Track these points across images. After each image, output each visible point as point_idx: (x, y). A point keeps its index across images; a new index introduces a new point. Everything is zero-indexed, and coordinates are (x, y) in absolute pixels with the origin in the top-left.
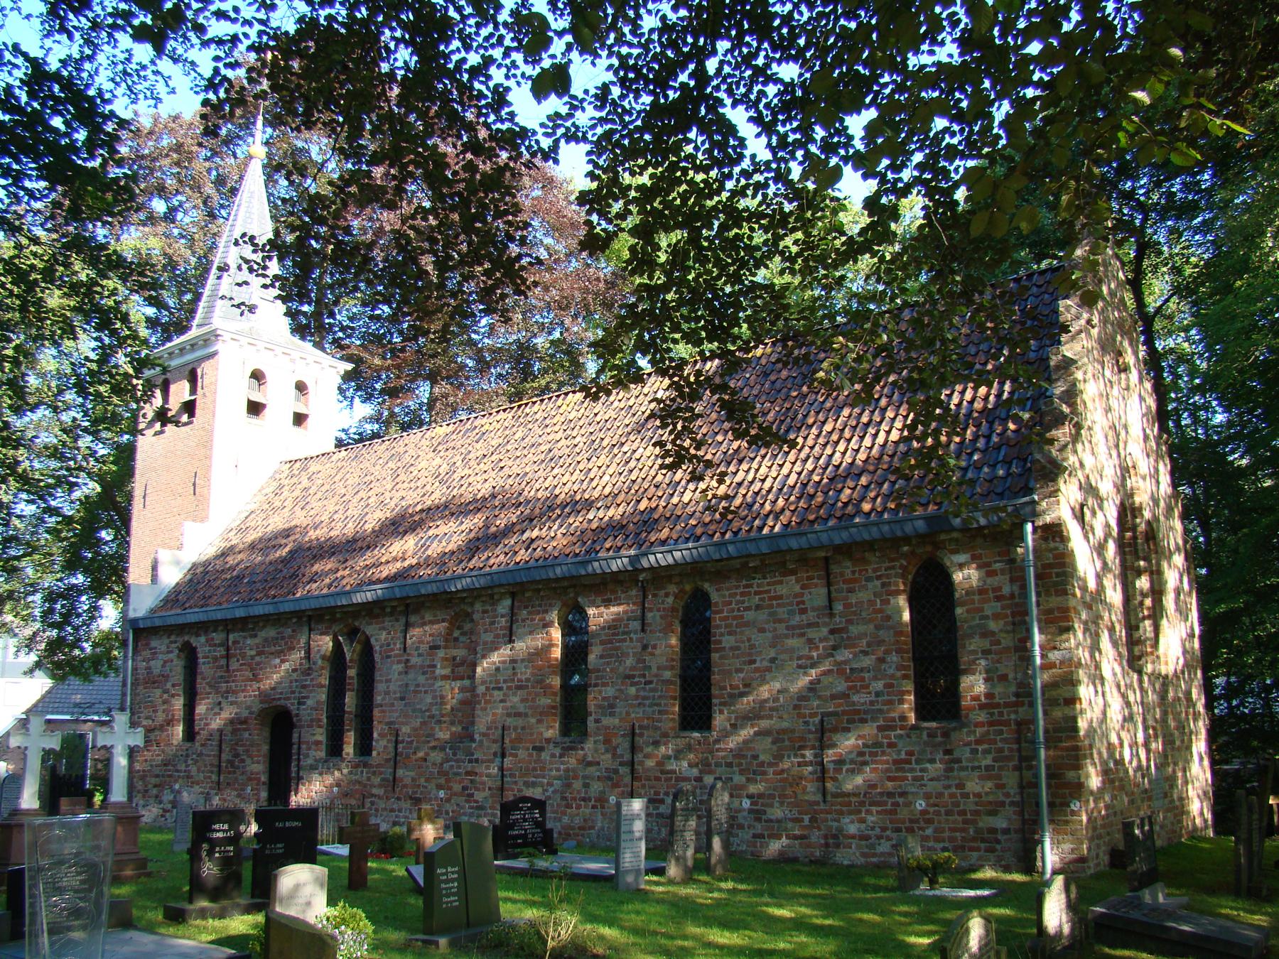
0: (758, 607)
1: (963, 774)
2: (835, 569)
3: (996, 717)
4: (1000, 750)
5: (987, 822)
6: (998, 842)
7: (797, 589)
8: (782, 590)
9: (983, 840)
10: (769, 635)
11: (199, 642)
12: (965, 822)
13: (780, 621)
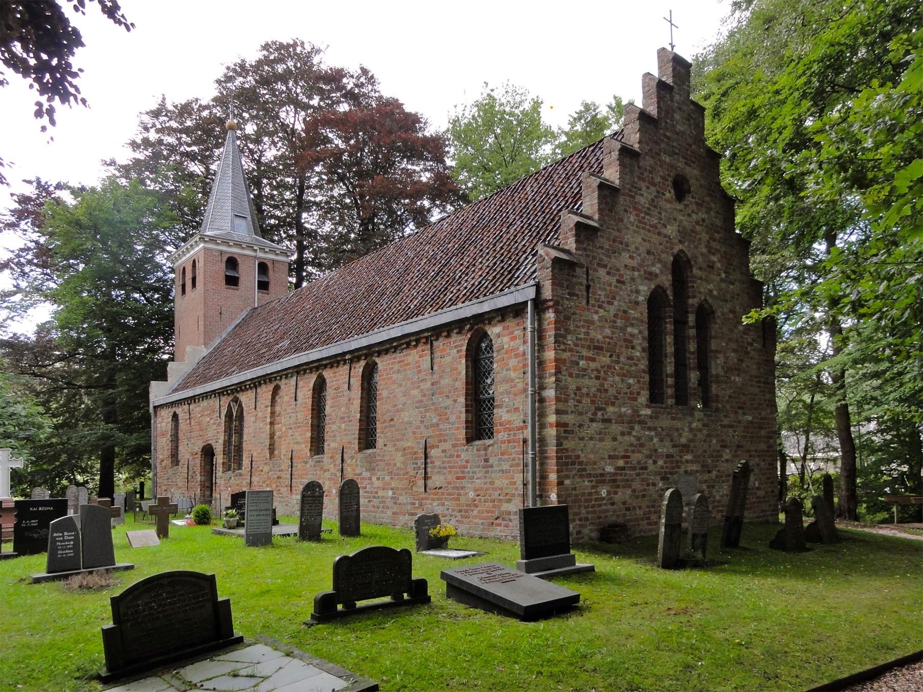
1: (493, 475)
3: (512, 437)
4: (514, 460)
5: (505, 507)
6: (510, 520)
9: (503, 519)
10: (403, 388)
11: (179, 410)
12: (494, 507)
13: (409, 379)
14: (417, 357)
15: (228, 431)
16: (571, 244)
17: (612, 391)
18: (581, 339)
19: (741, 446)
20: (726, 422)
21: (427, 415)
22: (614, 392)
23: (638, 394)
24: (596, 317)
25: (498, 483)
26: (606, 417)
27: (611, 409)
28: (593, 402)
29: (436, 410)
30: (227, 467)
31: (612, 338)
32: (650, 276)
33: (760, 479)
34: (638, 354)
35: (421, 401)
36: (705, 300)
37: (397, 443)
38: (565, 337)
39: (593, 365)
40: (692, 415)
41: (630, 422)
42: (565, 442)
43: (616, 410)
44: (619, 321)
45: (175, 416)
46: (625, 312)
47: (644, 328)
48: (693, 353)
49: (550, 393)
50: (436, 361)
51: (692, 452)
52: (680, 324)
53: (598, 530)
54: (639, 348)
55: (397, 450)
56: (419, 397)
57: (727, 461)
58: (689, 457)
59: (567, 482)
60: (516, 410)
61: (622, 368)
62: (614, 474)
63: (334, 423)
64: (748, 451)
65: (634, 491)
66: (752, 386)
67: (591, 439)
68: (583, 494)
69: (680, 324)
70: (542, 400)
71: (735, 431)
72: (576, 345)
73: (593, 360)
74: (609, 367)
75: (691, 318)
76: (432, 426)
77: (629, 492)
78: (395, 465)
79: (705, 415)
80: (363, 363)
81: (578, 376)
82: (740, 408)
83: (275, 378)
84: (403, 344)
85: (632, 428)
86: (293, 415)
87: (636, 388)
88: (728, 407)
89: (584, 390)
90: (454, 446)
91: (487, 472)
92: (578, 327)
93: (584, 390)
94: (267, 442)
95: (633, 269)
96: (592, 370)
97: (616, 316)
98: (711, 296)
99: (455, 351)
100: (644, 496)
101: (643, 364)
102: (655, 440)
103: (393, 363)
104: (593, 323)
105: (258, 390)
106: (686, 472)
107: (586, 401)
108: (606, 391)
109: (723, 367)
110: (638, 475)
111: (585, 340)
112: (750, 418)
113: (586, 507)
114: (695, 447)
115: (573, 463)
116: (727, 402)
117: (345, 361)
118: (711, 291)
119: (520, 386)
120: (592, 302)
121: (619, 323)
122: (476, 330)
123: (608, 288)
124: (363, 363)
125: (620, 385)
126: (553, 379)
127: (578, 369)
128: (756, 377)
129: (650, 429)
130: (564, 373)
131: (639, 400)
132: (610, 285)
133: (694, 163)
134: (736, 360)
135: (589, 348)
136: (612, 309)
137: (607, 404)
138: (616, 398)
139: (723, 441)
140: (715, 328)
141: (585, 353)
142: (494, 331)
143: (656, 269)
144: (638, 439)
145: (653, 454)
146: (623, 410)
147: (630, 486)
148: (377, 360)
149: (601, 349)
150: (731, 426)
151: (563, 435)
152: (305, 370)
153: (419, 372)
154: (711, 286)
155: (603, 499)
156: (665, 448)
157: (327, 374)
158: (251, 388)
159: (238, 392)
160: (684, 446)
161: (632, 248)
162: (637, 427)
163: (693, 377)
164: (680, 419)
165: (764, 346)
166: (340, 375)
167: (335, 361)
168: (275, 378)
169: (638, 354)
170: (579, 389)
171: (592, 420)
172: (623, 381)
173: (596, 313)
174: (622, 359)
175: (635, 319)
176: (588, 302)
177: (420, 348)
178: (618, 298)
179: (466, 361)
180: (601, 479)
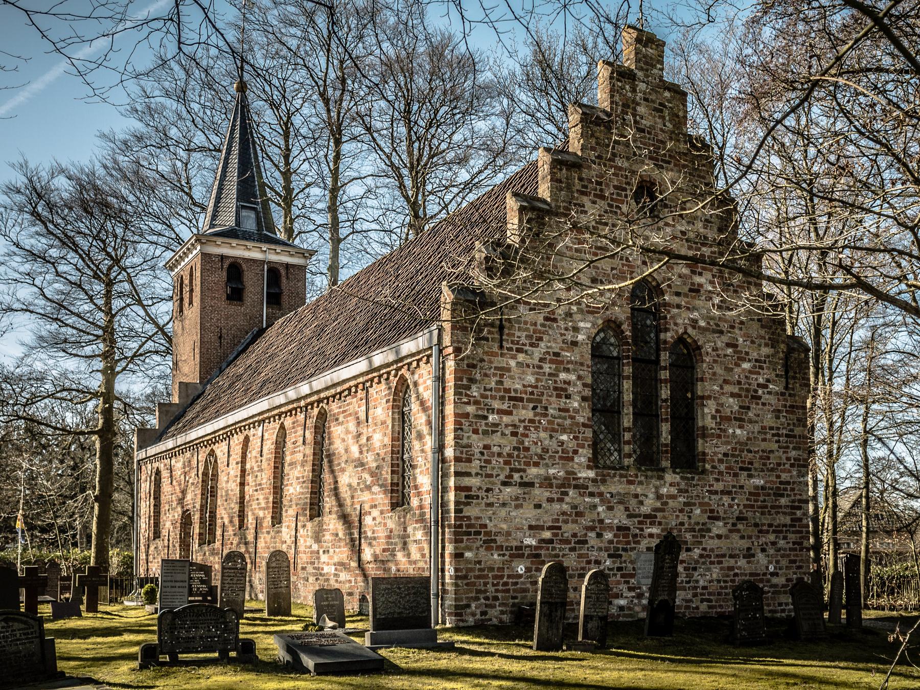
18: (491, 390)
19: (745, 519)
20: (719, 486)
22: (539, 451)
23: (576, 452)
24: (513, 363)
26: (525, 480)
27: (533, 471)
33: (777, 562)
34: (576, 405)
36: (686, 332)
39: (506, 419)
40: (661, 478)
41: (562, 486)
42: (465, 509)
43: (542, 471)
46: (557, 354)
48: (666, 401)
49: (449, 452)
50: (371, 412)
51: (660, 523)
53: (511, 612)
57: (719, 537)
59: (468, 554)
61: (549, 422)
62: (536, 548)
64: (756, 525)
66: (764, 440)
67: (504, 505)
68: (491, 569)
70: (444, 461)
71: (733, 499)
73: (509, 413)
79: (682, 478)
81: (485, 433)
87: (572, 445)
88: (722, 467)
89: (495, 449)
92: (486, 375)
93: (495, 449)
96: (506, 426)
97: (541, 360)
98: (694, 327)
102: (600, 509)
104: (509, 370)
108: (527, 449)
109: (714, 417)
110: (573, 549)
112: (761, 482)
113: (494, 585)
114: (664, 517)
115: (479, 533)
116: (721, 461)
118: (695, 321)
121: (547, 368)
123: (532, 328)
125: (547, 442)
127: (487, 424)
128: (771, 428)
129: (592, 495)
131: (576, 460)
132: (535, 324)
133: (669, 163)
134: (736, 408)
135: (502, 398)
136: (537, 353)
137: (527, 464)
138: (541, 457)
139: (712, 511)
141: (496, 405)
145: (598, 527)
146: (552, 471)
149: (521, 400)
150: (729, 493)
151: (463, 500)
154: (695, 315)
155: (520, 576)
156: (618, 517)
160: (646, 516)
164: (641, 483)
165: (786, 388)
169: (576, 405)
170: (486, 447)
171: (505, 484)
172: (551, 437)
173: (514, 357)
174: (551, 411)
176: (501, 347)
178: (545, 338)
180: (518, 552)
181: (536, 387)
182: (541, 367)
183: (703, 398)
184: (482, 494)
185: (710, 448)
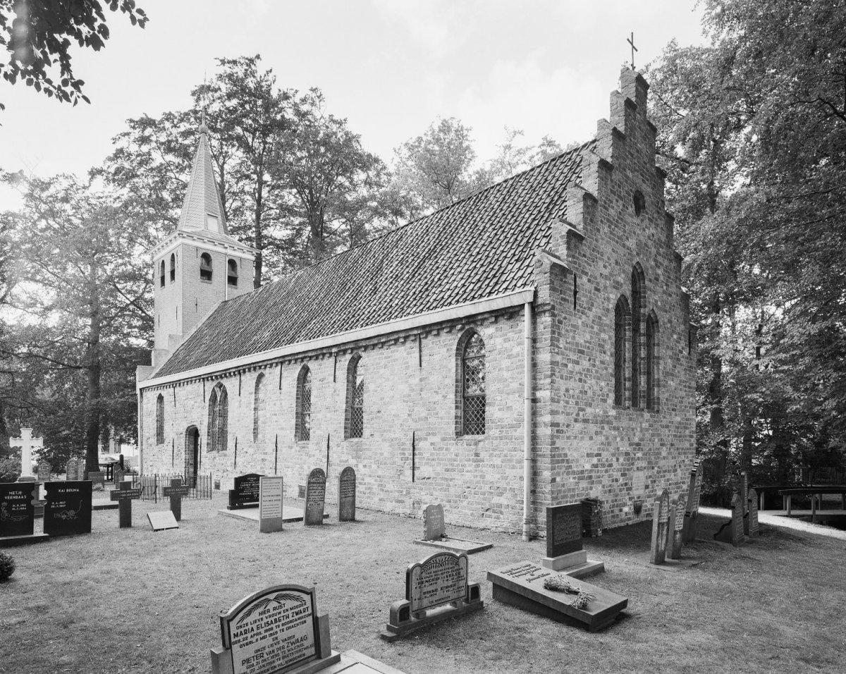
0: (385, 367)
2: (424, 341)
3: (504, 434)
6: (502, 513)
7: (405, 354)
8: (397, 355)
9: (494, 512)
14: (404, 354)
15: (212, 413)
16: (562, 251)
17: (590, 393)
21: (416, 409)
25: (489, 478)
27: (589, 410)
28: (577, 403)
29: (424, 405)
30: (212, 447)
31: (590, 343)
32: (617, 286)
34: (608, 358)
35: (410, 396)
37: (385, 434)
38: (558, 341)
39: (577, 368)
42: (557, 441)
44: (595, 327)
45: (160, 398)
47: (613, 334)
52: (636, 330)
54: (609, 354)
55: (384, 440)
56: (407, 392)
57: (664, 458)
58: (639, 455)
59: (558, 479)
60: (509, 408)
61: (597, 372)
62: (591, 471)
63: (318, 412)
65: (603, 486)
67: (575, 437)
68: (569, 490)
69: (636, 330)
72: (566, 349)
73: (577, 363)
74: (588, 370)
75: (643, 326)
76: (420, 419)
77: (600, 488)
78: (382, 454)
80: (348, 357)
82: (673, 410)
83: (260, 367)
84: (391, 340)
85: (603, 428)
86: (278, 403)
89: (571, 392)
90: (443, 439)
91: (478, 466)
92: (567, 331)
94: (252, 426)
95: (606, 278)
99: (445, 349)
100: (610, 490)
101: (611, 369)
102: (618, 439)
103: (379, 359)
105: (243, 378)
106: (638, 468)
107: (572, 401)
110: (606, 471)
111: (572, 344)
112: (678, 419)
117: (331, 354)
119: (515, 385)
120: (578, 307)
122: (468, 328)
124: (348, 357)
126: (549, 380)
130: (557, 374)
132: (590, 292)
136: (591, 314)
140: (658, 337)
141: (573, 357)
142: (486, 332)
143: (621, 279)
144: (607, 438)
146: (597, 410)
147: (600, 482)
148: (363, 354)
149: (582, 352)
150: (667, 427)
152: (290, 361)
153: (407, 368)
157: (312, 365)
158: (235, 375)
159: (222, 378)
160: (638, 444)
161: (605, 258)
162: (606, 427)
163: (643, 379)
165: (689, 353)
166: (325, 367)
167: (320, 354)
168: (260, 367)
170: (567, 390)
171: (576, 421)
174: (597, 363)
175: (606, 325)
176: (575, 307)
177: (408, 344)
179: (457, 360)
180: (581, 475)
181: (590, 343)
182: (593, 328)
183: (658, 358)
184: (565, 429)
185: (661, 394)
